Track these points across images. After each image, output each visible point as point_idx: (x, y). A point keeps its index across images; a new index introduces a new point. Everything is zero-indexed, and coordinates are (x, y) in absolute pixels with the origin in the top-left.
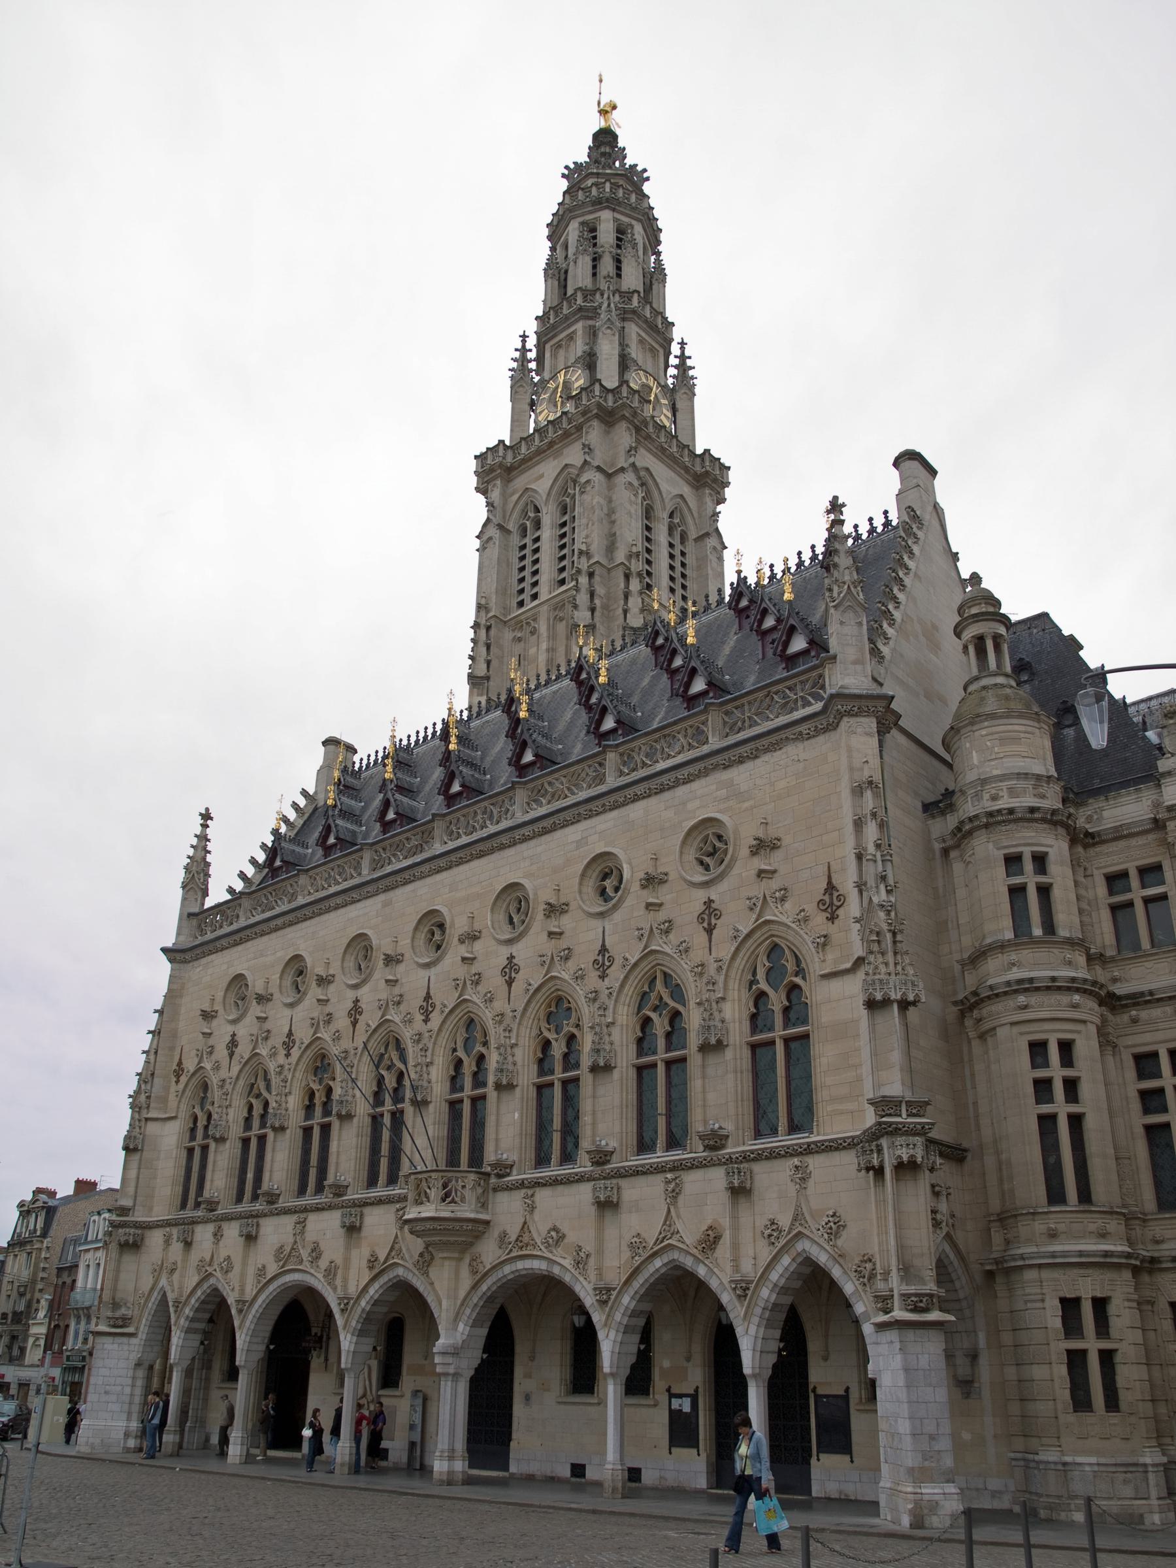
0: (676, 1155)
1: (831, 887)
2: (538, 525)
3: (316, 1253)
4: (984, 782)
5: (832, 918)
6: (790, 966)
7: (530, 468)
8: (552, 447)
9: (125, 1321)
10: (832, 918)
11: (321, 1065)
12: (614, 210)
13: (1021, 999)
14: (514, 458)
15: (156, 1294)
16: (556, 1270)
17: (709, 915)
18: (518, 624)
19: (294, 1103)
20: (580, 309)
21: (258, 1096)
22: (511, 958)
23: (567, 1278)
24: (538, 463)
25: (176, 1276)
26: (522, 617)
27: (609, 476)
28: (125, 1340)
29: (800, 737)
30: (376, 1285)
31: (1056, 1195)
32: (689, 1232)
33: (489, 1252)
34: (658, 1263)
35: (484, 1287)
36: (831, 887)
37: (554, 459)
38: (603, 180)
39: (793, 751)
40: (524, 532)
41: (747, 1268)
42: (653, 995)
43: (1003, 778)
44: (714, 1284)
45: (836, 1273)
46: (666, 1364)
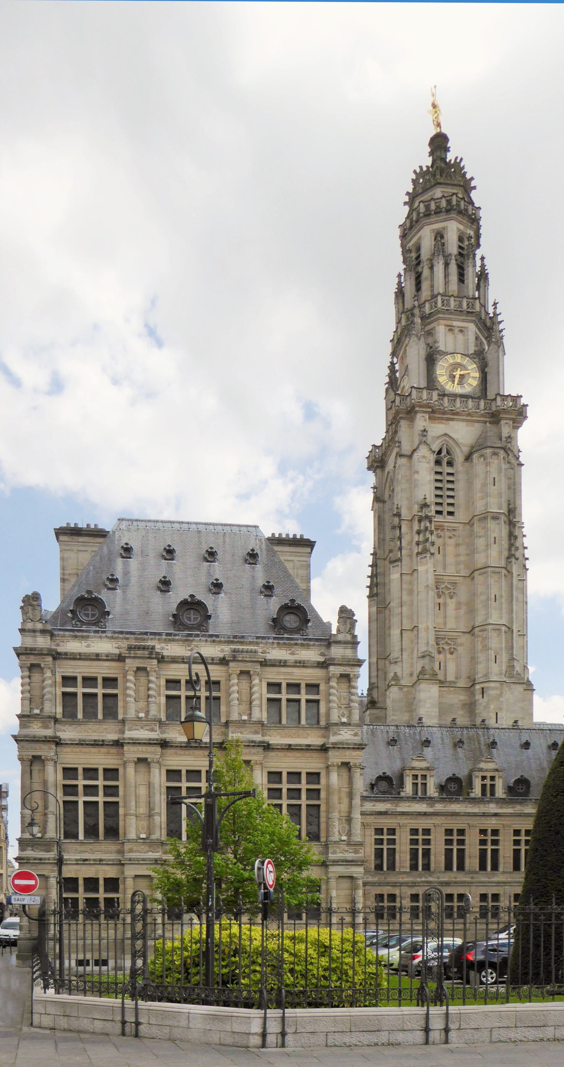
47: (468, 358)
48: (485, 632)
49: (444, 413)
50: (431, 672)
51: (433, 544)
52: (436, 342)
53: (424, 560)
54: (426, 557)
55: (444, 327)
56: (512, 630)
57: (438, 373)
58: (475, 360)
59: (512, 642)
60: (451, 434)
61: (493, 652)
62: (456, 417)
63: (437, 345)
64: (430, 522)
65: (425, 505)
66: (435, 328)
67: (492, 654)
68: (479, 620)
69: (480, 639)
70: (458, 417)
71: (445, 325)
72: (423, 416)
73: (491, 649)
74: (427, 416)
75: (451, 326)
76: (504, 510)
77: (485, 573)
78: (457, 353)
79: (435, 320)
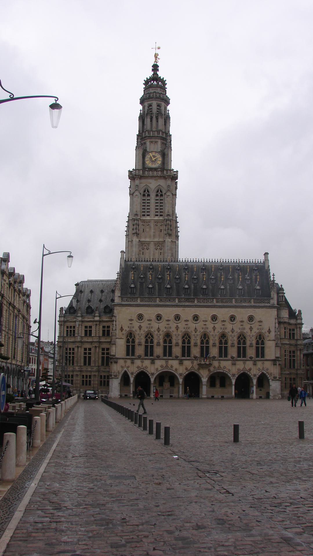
0: (244, 359)
1: (269, 329)
2: (149, 195)
3: (172, 367)
4: (283, 317)
5: (269, 333)
6: (262, 338)
7: (147, 179)
9: (116, 376)
10: (269, 333)
11: (168, 335)
12: (165, 103)
13: (285, 345)
15: (123, 371)
16: (225, 372)
17: (251, 329)
18: (144, 221)
19: (161, 341)
20: (161, 137)
21: (149, 338)
22: (214, 326)
23: (227, 373)
24: (150, 179)
25: (129, 368)
28: (117, 379)
29: (267, 308)
30: (188, 372)
31: (285, 367)
32: (247, 368)
33: (212, 369)
34: (242, 372)
35: (211, 373)
36: (269, 329)
37: (155, 180)
39: (264, 309)
40: (144, 195)
41: (255, 373)
42: (241, 338)
43: (285, 318)
44: (250, 374)
45: (267, 374)
46: (228, 383)
52: (146, 148)
64: (138, 221)
79: (146, 139)
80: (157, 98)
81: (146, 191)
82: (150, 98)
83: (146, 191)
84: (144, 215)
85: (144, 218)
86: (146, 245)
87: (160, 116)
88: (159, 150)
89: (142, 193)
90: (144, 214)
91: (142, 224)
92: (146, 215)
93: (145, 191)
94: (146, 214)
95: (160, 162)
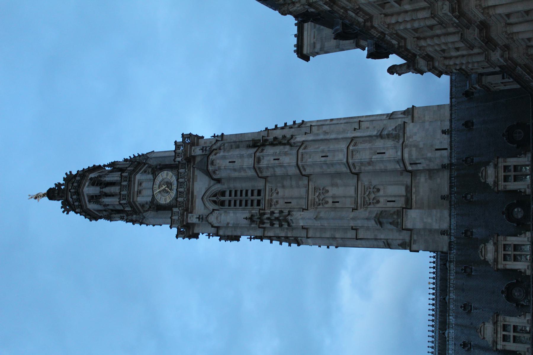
2: (223, 194)
8: (190, 181)
14: (183, 206)
26: (267, 198)
27: (222, 140)
38: (70, 193)
40: (222, 203)
47: (156, 180)
48: (356, 164)
49: (188, 200)
50: (395, 217)
51: (281, 212)
53: (294, 221)
54: (291, 220)
55: (138, 198)
56: (354, 137)
57: (164, 203)
58: (157, 175)
59: (365, 137)
60: (203, 194)
61: (374, 157)
62: (191, 190)
63: (149, 203)
64: (264, 214)
65: (251, 219)
66: (139, 204)
67: (375, 157)
68: (344, 169)
69: (363, 168)
70: (191, 188)
71: (137, 197)
72: (190, 218)
73: (371, 159)
74: (190, 215)
75: (138, 192)
76: (252, 151)
77: (303, 166)
78: (153, 188)
80: (79, 186)
81: (215, 199)
82: (79, 200)
83: (215, 199)
84: (259, 203)
85: (262, 202)
86: (317, 194)
87: (102, 179)
88: (150, 176)
89: (216, 207)
90: (255, 203)
91: (275, 204)
92: (259, 198)
93: (215, 202)
94: (256, 197)
95: (170, 173)
